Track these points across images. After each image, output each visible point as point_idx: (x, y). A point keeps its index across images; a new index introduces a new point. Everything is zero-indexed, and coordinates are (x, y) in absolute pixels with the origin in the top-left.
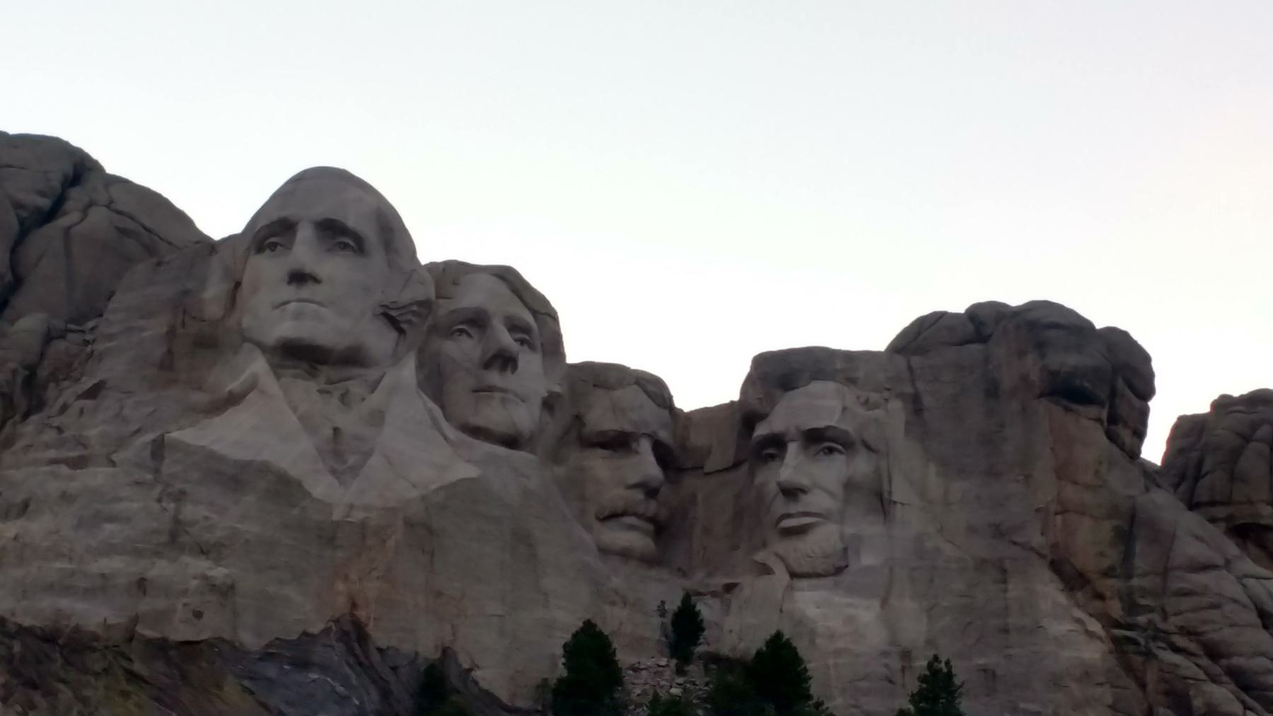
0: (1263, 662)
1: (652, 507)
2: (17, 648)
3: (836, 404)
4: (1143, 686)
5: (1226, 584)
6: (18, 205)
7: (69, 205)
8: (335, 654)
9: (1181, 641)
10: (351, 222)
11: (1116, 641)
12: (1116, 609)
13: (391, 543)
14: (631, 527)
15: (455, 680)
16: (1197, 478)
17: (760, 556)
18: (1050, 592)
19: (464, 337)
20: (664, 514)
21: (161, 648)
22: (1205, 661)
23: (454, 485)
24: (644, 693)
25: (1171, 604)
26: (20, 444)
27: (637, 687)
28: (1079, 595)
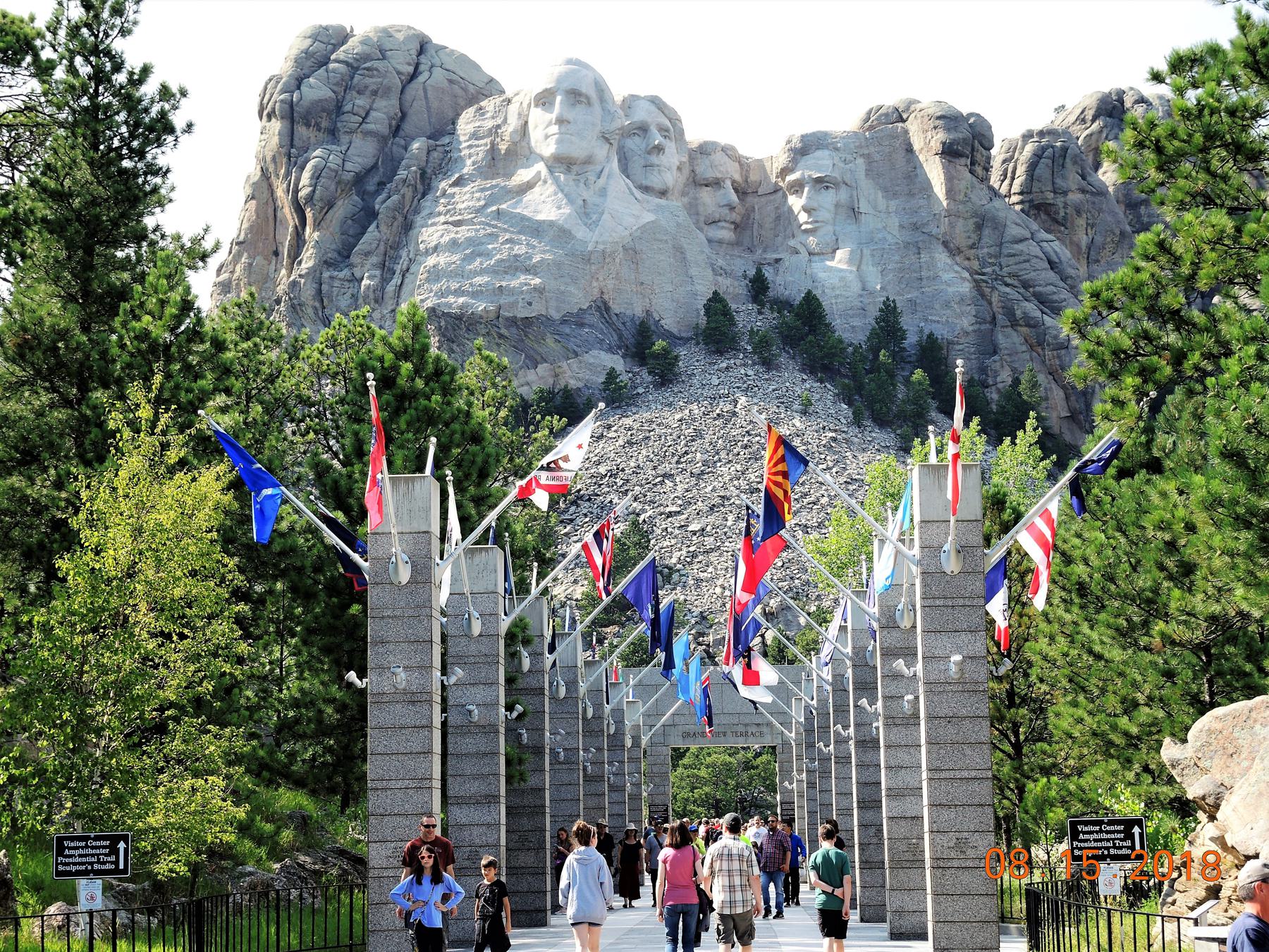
0: (1051, 288)
1: (735, 216)
2: (443, 324)
3: (829, 162)
4: (990, 303)
5: (1032, 248)
6: (399, 73)
7: (422, 68)
8: (594, 318)
9: (1008, 280)
10: (584, 91)
11: (975, 281)
12: (975, 265)
13: (617, 260)
14: (723, 228)
15: (653, 328)
16: (1013, 179)
17: (792, 243)
18: (942, 257)
19: (636, 138)
20: (738, 219)
21: (513, 322)
22: (1022, 290)
23: (644, 226)
24: (744, 326)
25: (1004, 261)
26: (425, 213)
27: (741, 320)
28: (957, 258)
